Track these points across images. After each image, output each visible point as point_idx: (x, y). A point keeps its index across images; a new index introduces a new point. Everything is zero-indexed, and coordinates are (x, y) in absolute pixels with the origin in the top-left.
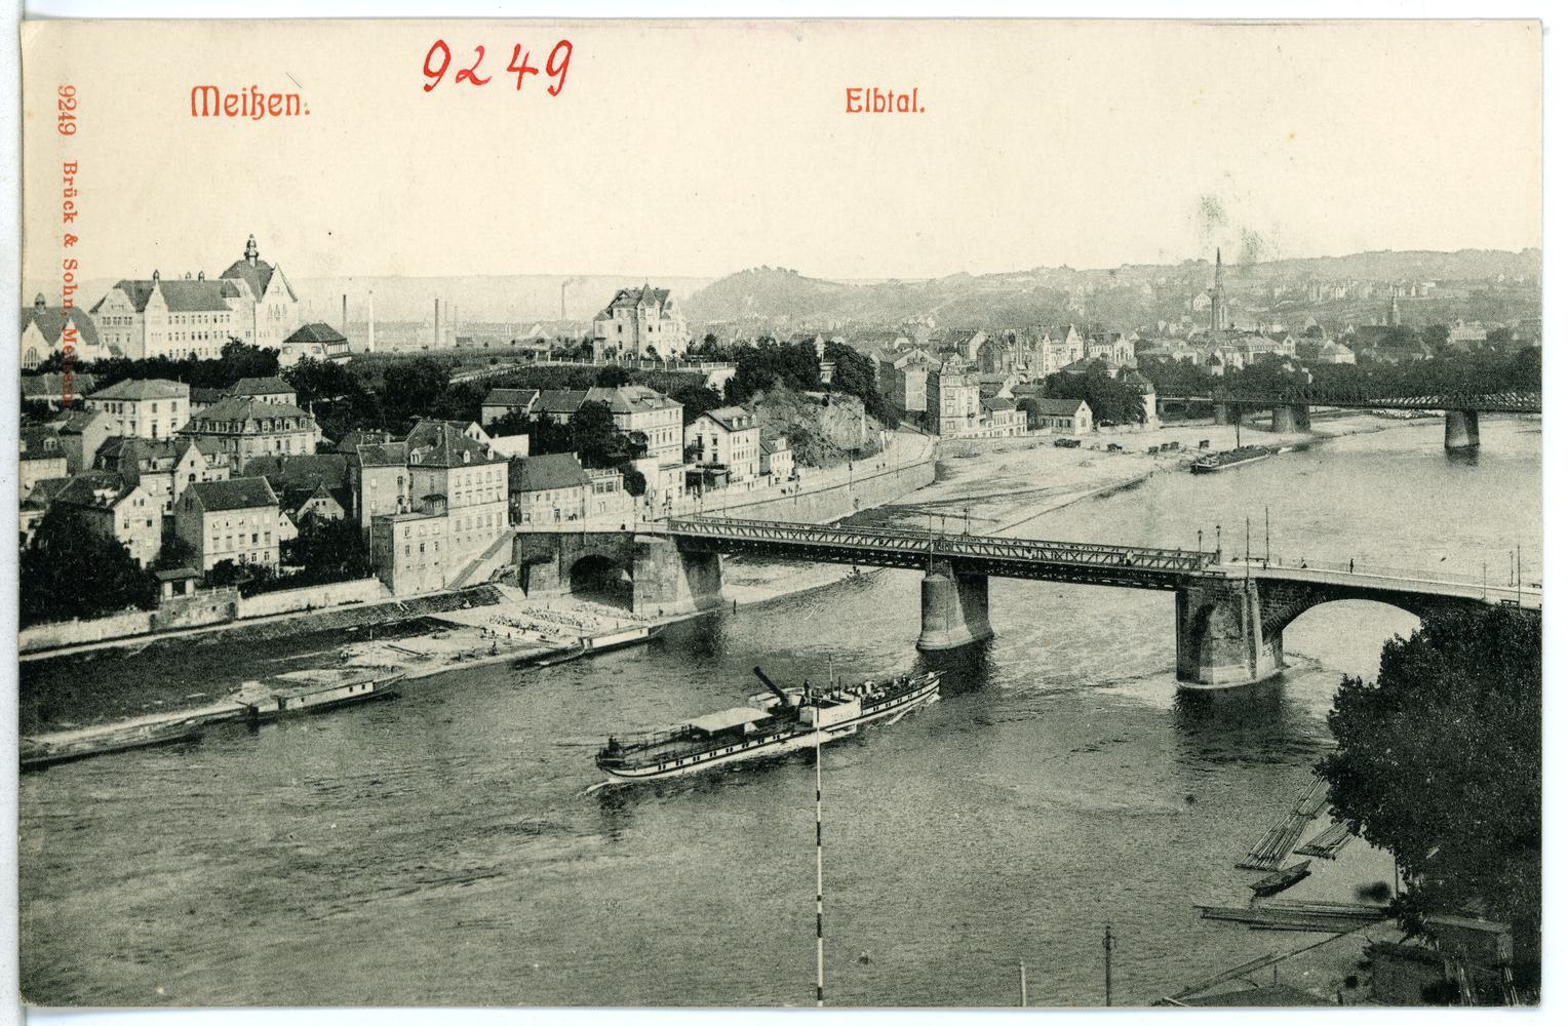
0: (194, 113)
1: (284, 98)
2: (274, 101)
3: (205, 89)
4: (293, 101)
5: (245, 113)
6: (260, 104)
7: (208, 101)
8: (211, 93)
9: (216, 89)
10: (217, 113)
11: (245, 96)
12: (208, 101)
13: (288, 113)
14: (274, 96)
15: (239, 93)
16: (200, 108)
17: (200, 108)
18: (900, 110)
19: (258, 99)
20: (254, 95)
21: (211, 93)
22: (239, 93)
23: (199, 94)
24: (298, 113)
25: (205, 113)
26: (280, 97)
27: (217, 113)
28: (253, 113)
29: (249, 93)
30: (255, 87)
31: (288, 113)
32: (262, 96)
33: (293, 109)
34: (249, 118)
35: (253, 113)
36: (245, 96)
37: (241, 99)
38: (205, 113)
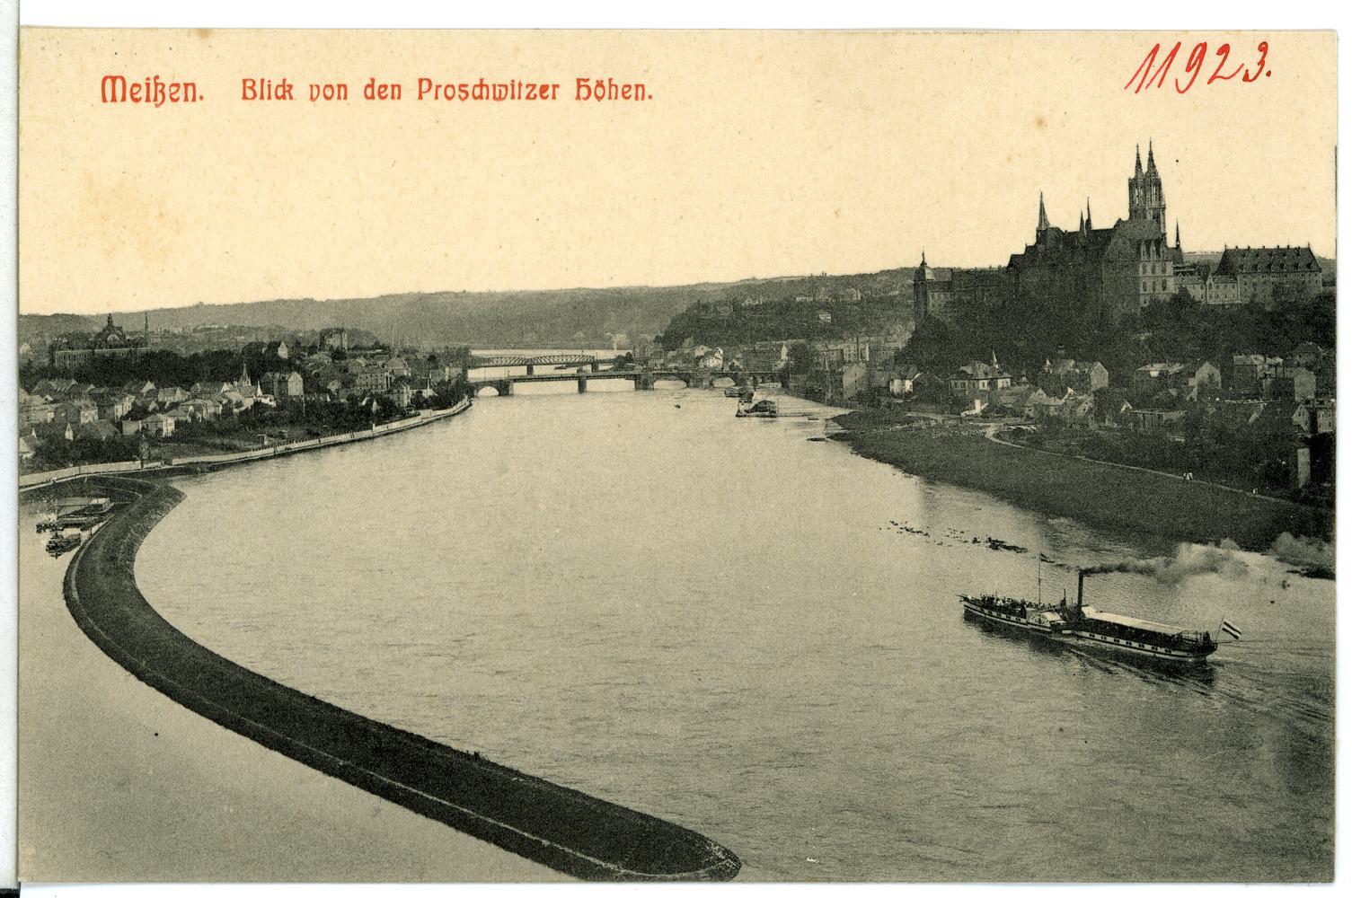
0: (104, 100)
1: (182, 89)
2: (174, 89)
3: (114, 79)
4: (190, 88)
5: (148, 100)
6: (162, 91)
7: (115, 88)
8: (119, 82)
9: (123, 79)
10: (124, 99)
11: (148, 85)
12: (115, 88)
13: (186, 99)
14: (625, 86)
15: (143, 82)
16: (109, 96)
17: (109, 96)
18: (278, 97)
19: (160, 87)
20: (156, 85)
21: (119, 82)
22: (143, 82)
23: (109, 83)
24: (194, 100)
25: (114, 99)
26: (629, 86)
27: (124, 99)
28: (156, 99)
29: (152, 82)
30: (157, 77)
31: (186, 99)
32: (163, 85)
33: (396, 96)
34: (152, 104)
35: (156, 99)
36: (148, 85)
37: (144, 87)
38: (114, 99)
